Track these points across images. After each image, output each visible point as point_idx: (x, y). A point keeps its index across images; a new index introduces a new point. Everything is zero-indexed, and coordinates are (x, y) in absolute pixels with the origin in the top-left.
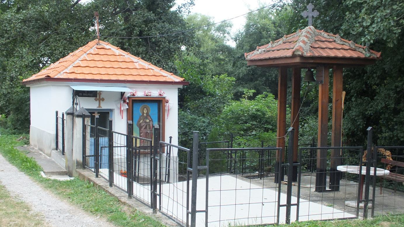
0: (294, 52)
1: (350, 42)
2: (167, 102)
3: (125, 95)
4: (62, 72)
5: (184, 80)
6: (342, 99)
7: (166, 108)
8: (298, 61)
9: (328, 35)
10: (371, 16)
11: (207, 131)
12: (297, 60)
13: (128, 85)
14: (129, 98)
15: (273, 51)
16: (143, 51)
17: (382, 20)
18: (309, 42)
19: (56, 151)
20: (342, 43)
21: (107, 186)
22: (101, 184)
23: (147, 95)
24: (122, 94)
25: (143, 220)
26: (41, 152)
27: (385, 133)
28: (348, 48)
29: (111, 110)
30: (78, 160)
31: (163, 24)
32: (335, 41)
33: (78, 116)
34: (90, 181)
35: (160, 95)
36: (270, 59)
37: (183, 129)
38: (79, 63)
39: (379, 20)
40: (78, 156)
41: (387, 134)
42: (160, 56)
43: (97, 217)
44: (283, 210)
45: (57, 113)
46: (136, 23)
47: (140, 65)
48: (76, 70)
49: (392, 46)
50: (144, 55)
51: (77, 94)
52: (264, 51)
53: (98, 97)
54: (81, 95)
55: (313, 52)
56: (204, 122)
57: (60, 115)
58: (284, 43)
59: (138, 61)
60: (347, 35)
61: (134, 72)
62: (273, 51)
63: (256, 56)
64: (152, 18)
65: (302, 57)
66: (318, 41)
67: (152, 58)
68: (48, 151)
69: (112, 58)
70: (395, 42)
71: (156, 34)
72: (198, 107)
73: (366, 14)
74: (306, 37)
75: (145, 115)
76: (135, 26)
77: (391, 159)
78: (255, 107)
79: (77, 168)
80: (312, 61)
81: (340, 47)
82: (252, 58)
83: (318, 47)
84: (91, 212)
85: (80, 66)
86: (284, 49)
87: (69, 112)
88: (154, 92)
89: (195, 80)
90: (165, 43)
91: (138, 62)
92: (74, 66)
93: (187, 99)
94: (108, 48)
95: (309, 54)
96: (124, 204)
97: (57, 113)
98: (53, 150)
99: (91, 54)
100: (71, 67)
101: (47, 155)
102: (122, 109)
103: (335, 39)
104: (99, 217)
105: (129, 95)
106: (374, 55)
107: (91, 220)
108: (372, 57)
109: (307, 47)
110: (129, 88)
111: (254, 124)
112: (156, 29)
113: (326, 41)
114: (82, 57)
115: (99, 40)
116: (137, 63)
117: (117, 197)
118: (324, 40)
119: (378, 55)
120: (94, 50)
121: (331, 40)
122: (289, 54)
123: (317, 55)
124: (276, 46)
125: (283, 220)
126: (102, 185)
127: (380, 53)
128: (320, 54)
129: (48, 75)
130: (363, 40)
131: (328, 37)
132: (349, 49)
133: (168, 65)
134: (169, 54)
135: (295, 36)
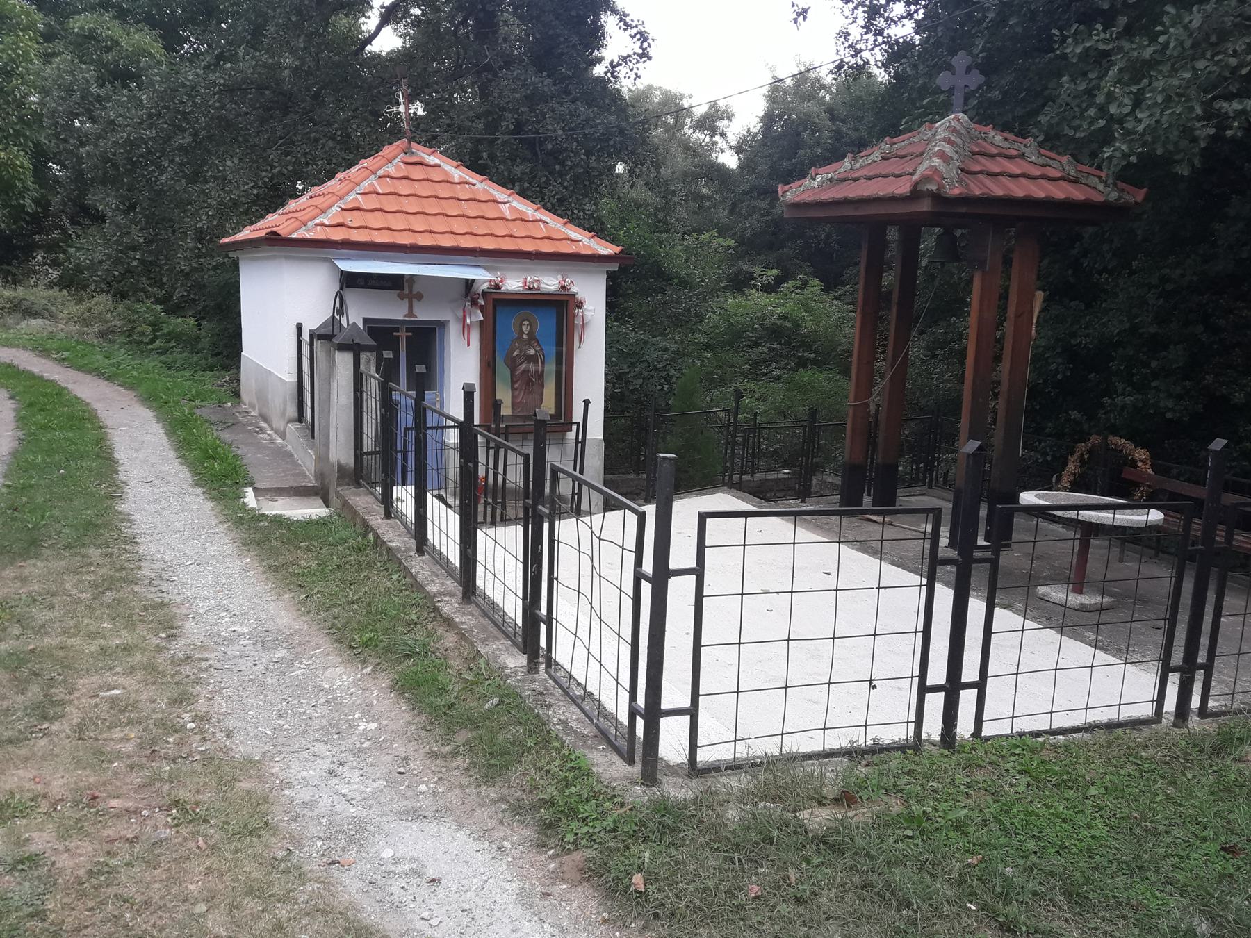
0: (916, 184)
1: (1065, 159)
2: (580, 305)
3: (475, 286)
4: (311, 224)
5: (622, 251)
6: (1032, 312)
7: (578, 322)
8: (925, 209)
9: (1006, 139)
10: (1134, 89)
11: (672, 372)
12: (925, 206)
13: (482, 260)
14: (484, 293)
15: (855, 180)
16: (523, 174)
17: (1168, 99)
18: (956, 156)
19: (298, 425)
20: (1041, 160)
21: (408, 549)
22: (394, 544)
23: (530, 289)
24: (469, 284)
25: (496, 700)
26: (263, 424)
27: (1123, 394)
28: (1058, 175)
29: (442, 325)
30: (343, 462)
31: (572, 107)
32: (1023, 156)
33: (342, 348)
34: (367, 528)
35: (563, 287)
36: (846, 202)
37: (616, 365)
38: (356, 199)
39: (1159, 99)
40: (341, 452)
41: (1129, 400)
42: (564, 187)
43: (365, 671)
44: (935, 702)
45: (299, 327)
46: (507, 100)
47: (512, 209)
48: (349, 219)
49: (1186, 174)
50: (526, 185)
51: (350, 281)
52: (830, 180)
53: (406, 291)
54: (363, 284)
55: (967, 185)
56: (666, 350)
57: (306, 337)
58: (884, 159)
59: (510, 199)
60: (1052, 141)
61: (500, 229)
62: (855, 180)
63: (808, 193)
64: (546, 90)
65: (937, 197)
66: (978, 153)
67: (545, 191)
68: (279, 423)
69: (443, 191)
70: (1197, 162)
71: (555, 131)
72: (651, 313)
73: (1119, 81)
74: (950, 142)
75: (525, 337)
76: (503, 109)
77: (1150, 471)
78: (779, 310)
79: (338, 485)
80: (963, 210)
81: (1039, 173)
82: (797, 199)
83: (981, 172)
84: (351, 647)
85: (358, 209)
86: (885, 176)
87: (322, 331)
88: (550, 283)
89: (645, 246)
90: (577, 154)
91: (508, 202)
92: (343, 206)
93: (627, 289)
94: (432, 163)
95: (956, 191)
96: (449, 623)
97: (299, 327)
98: (290, 421)
99: (388, 177)
100: (335, 209)
101: (276, 432)
102: (468, 321)
103: (1023, 149)
104: (369, 669)
105: (485, 286)
106: (1127, 197)
107: (345, 678)
108: (1122, 200)
109: (951, 172)
110: (486, 268)
111: (774, 349)
112: (555, 119)
113: (999, 155)
114: (365, 184)
115: (409, 142)
116: (508, 205)
117: (429, 597)
118: (995, 151)
119: (1140, 195)
120: (397, 167)
121: (1015, 153)
122: (902, 187)
123: (977, 192)
124: (862, 167)
125: (933, 728)
126: (397, 548)
127: (1145, 189)
128: (986, 191)
129: (275, 229)
130: (1106, 155)
131: (1006, 145)
132: (1062, 178)
133: (583, 210)
134: (587, 183)
135: (915, 140)
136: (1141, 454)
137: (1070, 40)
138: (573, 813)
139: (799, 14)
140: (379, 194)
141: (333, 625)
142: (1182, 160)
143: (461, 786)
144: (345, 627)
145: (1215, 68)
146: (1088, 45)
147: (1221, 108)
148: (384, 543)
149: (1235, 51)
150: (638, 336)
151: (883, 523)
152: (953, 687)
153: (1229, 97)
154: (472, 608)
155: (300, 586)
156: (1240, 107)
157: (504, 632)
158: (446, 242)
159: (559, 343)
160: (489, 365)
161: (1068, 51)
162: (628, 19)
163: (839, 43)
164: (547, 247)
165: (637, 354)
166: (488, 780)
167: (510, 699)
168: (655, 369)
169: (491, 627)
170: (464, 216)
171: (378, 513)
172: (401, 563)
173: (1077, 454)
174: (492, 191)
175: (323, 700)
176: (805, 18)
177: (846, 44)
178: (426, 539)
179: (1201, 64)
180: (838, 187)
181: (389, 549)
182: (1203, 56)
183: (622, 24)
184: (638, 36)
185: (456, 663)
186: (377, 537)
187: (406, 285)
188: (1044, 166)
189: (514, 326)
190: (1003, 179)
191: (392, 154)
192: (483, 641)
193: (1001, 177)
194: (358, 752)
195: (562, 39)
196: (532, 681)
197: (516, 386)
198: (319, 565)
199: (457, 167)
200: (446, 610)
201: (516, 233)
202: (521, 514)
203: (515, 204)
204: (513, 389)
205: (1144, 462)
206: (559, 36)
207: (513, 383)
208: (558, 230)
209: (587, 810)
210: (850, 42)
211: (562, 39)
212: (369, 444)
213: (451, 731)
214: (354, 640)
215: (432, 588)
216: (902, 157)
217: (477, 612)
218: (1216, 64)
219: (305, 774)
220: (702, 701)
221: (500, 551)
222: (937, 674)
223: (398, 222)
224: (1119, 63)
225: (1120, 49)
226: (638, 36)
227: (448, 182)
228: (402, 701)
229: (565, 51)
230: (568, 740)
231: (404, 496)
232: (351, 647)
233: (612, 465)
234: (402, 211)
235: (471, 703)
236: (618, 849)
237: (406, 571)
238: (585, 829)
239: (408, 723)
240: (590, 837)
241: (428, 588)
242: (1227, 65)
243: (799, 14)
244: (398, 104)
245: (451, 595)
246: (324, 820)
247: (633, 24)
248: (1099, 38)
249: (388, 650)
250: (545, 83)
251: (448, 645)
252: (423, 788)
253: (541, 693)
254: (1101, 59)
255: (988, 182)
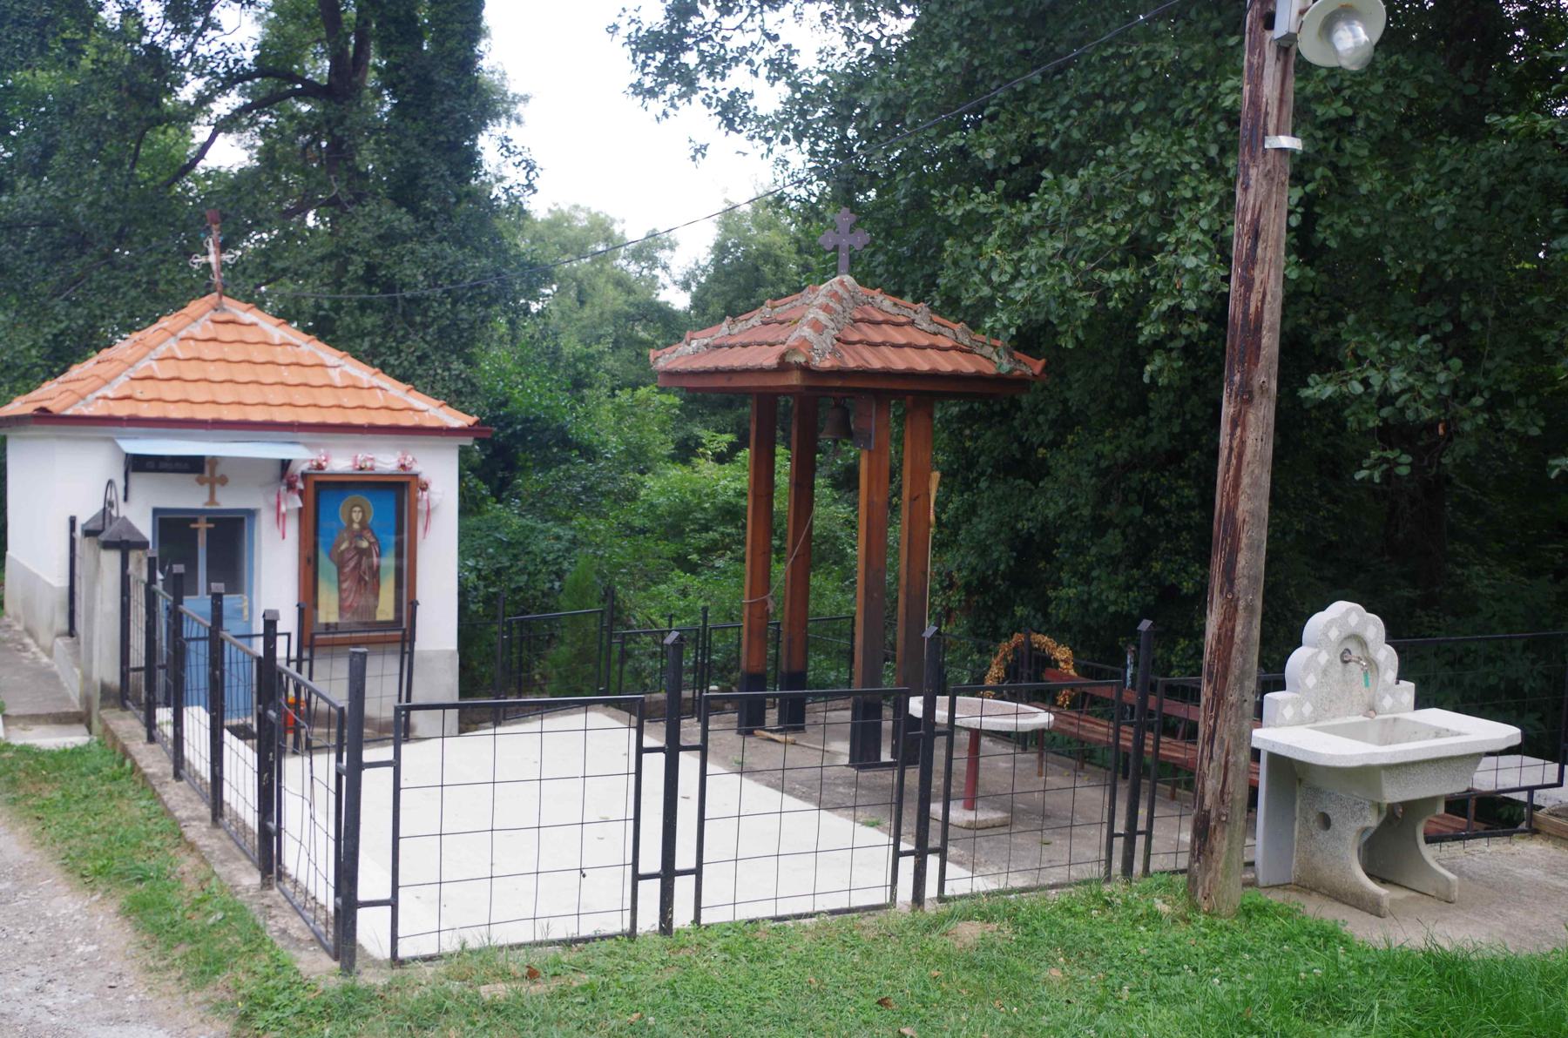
0: (783, 356)
1: (958, 327)
2: (424, 487)
3: (292, 467)
4: (90, 397)
5: (476, 423)
6: (928, 495)
7: (422, 507)
8: (795, 383)
9: (895, 304)
10: (1016, 255)
11: (566, 565)
12: (794, 379)
13: (302, 436)
14: (304, 476)
15: (731, 347)
16: (373, 326)
17: (1041, 270)
18: (831, 325)
19: (68, 640)
20: (933, 328)
21: (165, 775)
22: (150, 771)
23: (361, 469)
24: (285, 464)
25: (220, 915)
26: (28, 640)
27: (1069, 586)
28: (949, 344)
29: (252, 513)
30: (108, 680)
31: (437, 248)
32: (912, 323)
33: (107, 545)
34: (126, 753)
35: (403, 466)
36: (717, 372)
37: (493, 558)
38: (149, 367)
39: (1034, 269)
40: (106, 670)
41: (1072, 592)
42: (426, 342)
43: (94, 898)
44: (650, 891)
45: (73, 521)
46: (355, 241)
47: (344, 374)
48: (140, 390)
49: (1070, 346)
50: (378, 340)
51: (137, 464)
52: (707, 346)
53: (207, 474)
54: (153, 466)
55: (842, 357)
56: (558, 538)
57: (78, 533)
58: (765, 324)
59: (342, 362)
60: (951, 306)
61: (326, 398)
62: (731, 347)
63: (683, 360)
64: (405, 228)
65: (806, 370)
66: (861, 320)
67: (402, 347)
68: (46, 638)
69: (259, 354)
70: (1080, 333)
71: (415, 276)
72: (543, 493)
73: (1000, 247)
74: (826, 308)
75: (356, 526)
76: (353, 251)
77: (1072, 672)
78: (733, 485)
79: (102, 708)
80: (838, 383)
81: (926, 343)
82: (669, 367)
83: (860, 342)
84: (83, 876)
85: (151, 378)
86: (760, 344)
87: (91, 527)
88: (386, 460)
89: (547, 407)
90: (441, 303)
91: (338, 366)
92: (133, 375)
93: (526, 461)
94: (247, 322)
95: (824, 362)
96: (192, 847)
97: (73, 521)
98: (59, 635)
99: (192, 338)
100: (123, 379)
101: (43, 649)
102: (283, 508)
103: (913, 315)
104: (98, 897)
105: (304, 467)
106: (1024, 369)
107: (71, 905)
108: (1018, 373)
109: (826, 341)
110: (306, 445)
111: (729, 535)
112: (415, 262)
113: (886, 322)
115: (220, 297)
116: (338, 370)
117: (177, 822)
118: (880, 317)
119: (1037, 366)
120: (204, 328)
121: (902, 319)
122: (769, 359)
123: (851, 364)
124: (740, 332)
125: (649, 919)
126: (153, 775)
127: (1043, 361)
128: (861, 363)
129: (45, 404)
130: (988, 325)
131: (894, 310)
132: (954, 348)
133: (449, 369)
134: (455, 337)
135: (798, 303)
136: (1062, 653)
137: (951, 202)
138: (266, 1004)
139: (697, 151)
140: (178, 359)
141: (68, 856)
142: (1067, 331)
143: (170, 994)
144: (79, 856)
145: (1093, 237)
146: (968, 207)
147: (1101, 278)
148: (140, 769)
149: (1114, 220)
150: (524, 522)
151: (786, 743)
152: (668, 873)
153: (1111, 267)
154: (220, 832)
155: (38, 818)
156: (1118, 278)
157: (245, 852)
158: (257, 415)
159: (399, 531)
160: (309, 561)
161: (949, 213)
162: (511, 145)
163: (778, 172)
164: (383, 419)
165: (521, 543)
166: (199, 986)
167: (236, 913)
168: (544, 562)
169: (236, 850)
170: (282, 384)
171: (141, 738)
172: (154, 790)
173: (1000, 655)
174: (321, 354)
175: (42, 928)
176: (704, 155)
177: (786, 174)
178: (182, 756)
179: (1081, 232)
180: (713, 354)
181: (144, 776)
182: (1085, 224)
183: (504, 150)
184: (524, 164)
185: (190, 884)
186: (134, 763)
187: (207, 468)
188: (935, 334)
189: (355, 512)
190: (884, 349)
191: (198, 312)
192: (222, 862)
193: (882, 348)
194: (71, 972)
195: (427, 169)
196: (263, 897)
197: (345, 586)
198: (64, 796)
199: (278, 325)
200: (191, 834)
201: (346, 402)
202: (333, 742)
203: (347, 368)
204: (340, 590)
205: (1066, 661)
206: (423, 165)
207: (340, 582)
208: (399, 399)
209: (279, 999)
210: (790, 172)
211: (427, 169)
212: (138, 657)
213: (170, 947)
214: (86, 869)
215: (181, 813)
216: (781, 323)
217: (224, 836)
218: (1096, 232)
219: (9, 990)
220: (401, 891)
221: (241, 763)
222: (651, 860)
223: (198, 393)
224: (1000, 226)
225: (1000, 213)
226: (524, 164)
227: (266, 343)
228: (127, 924)
229: (431, 182)
230: (279, 944)
231: (197, 720)
232: (83, 876)
233: (469, 680)
234: (206, 380)
235: (197, 919)
236: (301, 1029)
237: (156, 797)
238: (276, 1015)
239: (130, 943)
240: (279, 1022)
241: (177, 814)
242: (1106, 235)
243: (697, 151)
244: (207, 254)
245: (201, 819)
246: (21, 1029)
247: (518, 151)
248: (982, 201)
249: (121, 875)
250: (404, 220)
251: (186, 869)
252: (131, 998)
253: (269, 906)
254: (978, 223)
255: (867, 353)
